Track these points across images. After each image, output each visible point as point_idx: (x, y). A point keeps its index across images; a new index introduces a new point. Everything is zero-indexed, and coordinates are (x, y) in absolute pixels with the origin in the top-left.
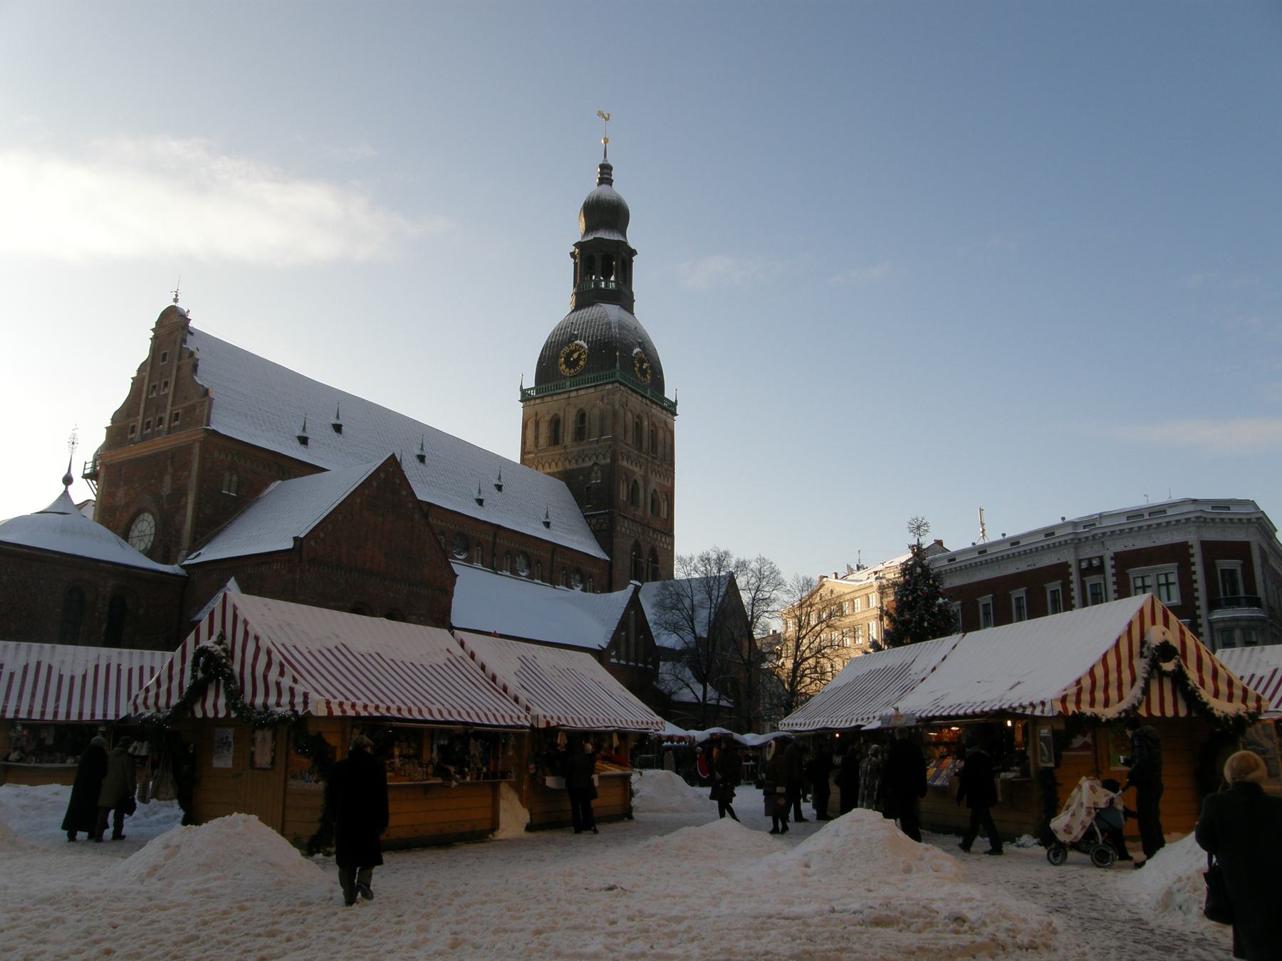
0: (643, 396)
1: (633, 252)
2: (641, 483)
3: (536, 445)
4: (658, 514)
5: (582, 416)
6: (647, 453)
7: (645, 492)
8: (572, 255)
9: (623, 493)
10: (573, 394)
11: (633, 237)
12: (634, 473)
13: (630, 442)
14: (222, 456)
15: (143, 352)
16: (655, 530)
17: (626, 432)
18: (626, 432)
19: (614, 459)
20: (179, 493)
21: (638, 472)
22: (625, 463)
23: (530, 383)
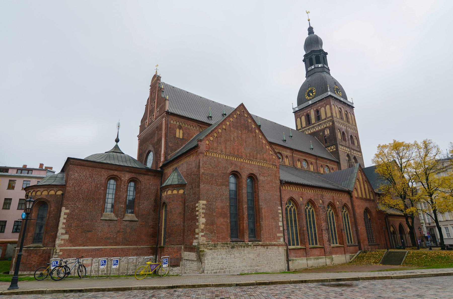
1: (326, 54)
3: (302, 127)
4: (354, 144)
5: (317, 112)
7: (348, 136)
8: (304, 61)
9: (339, 136)
11: (325, 48)
13: (338, 117)
14: (175, 123)
15: (148, 95)
17: (336, 114)
18: (336, 114)
19: (333, 123)
20: (160, 140)
23: (295, 105)
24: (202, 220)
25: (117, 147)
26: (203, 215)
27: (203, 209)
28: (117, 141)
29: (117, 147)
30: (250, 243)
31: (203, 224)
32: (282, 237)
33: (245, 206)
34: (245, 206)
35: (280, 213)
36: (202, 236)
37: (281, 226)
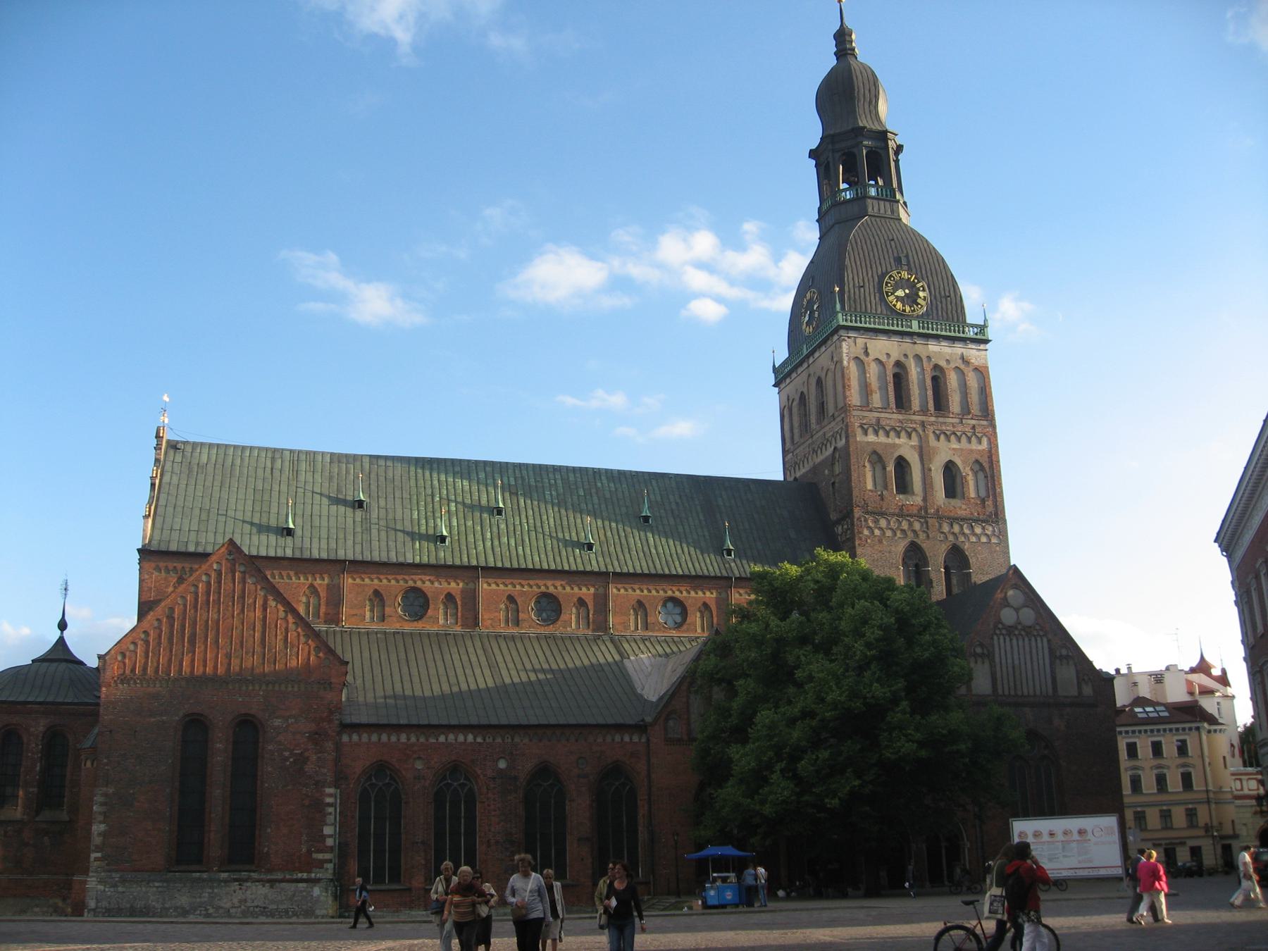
0: (902, 334)
2: (913, 459)
6: (924, 411)
7: (926, 472)
10: (811, 360)
11: (889, 111)
12: (894, 446)
16: (953, 520)
21: (906, 447)
22: (871, 438)
24: (98, 828)
25: (61, 642)
26: (101, 818)
27: (102, 804)
28: (63, 625)
29: (61, 642)
30: (224, 875)
31: (99, 834)
32: (330, 861)
33: (217, 792)
34: (217, 792)
35: (329, 805)
36: (96, 859)
37: (330, 836)
